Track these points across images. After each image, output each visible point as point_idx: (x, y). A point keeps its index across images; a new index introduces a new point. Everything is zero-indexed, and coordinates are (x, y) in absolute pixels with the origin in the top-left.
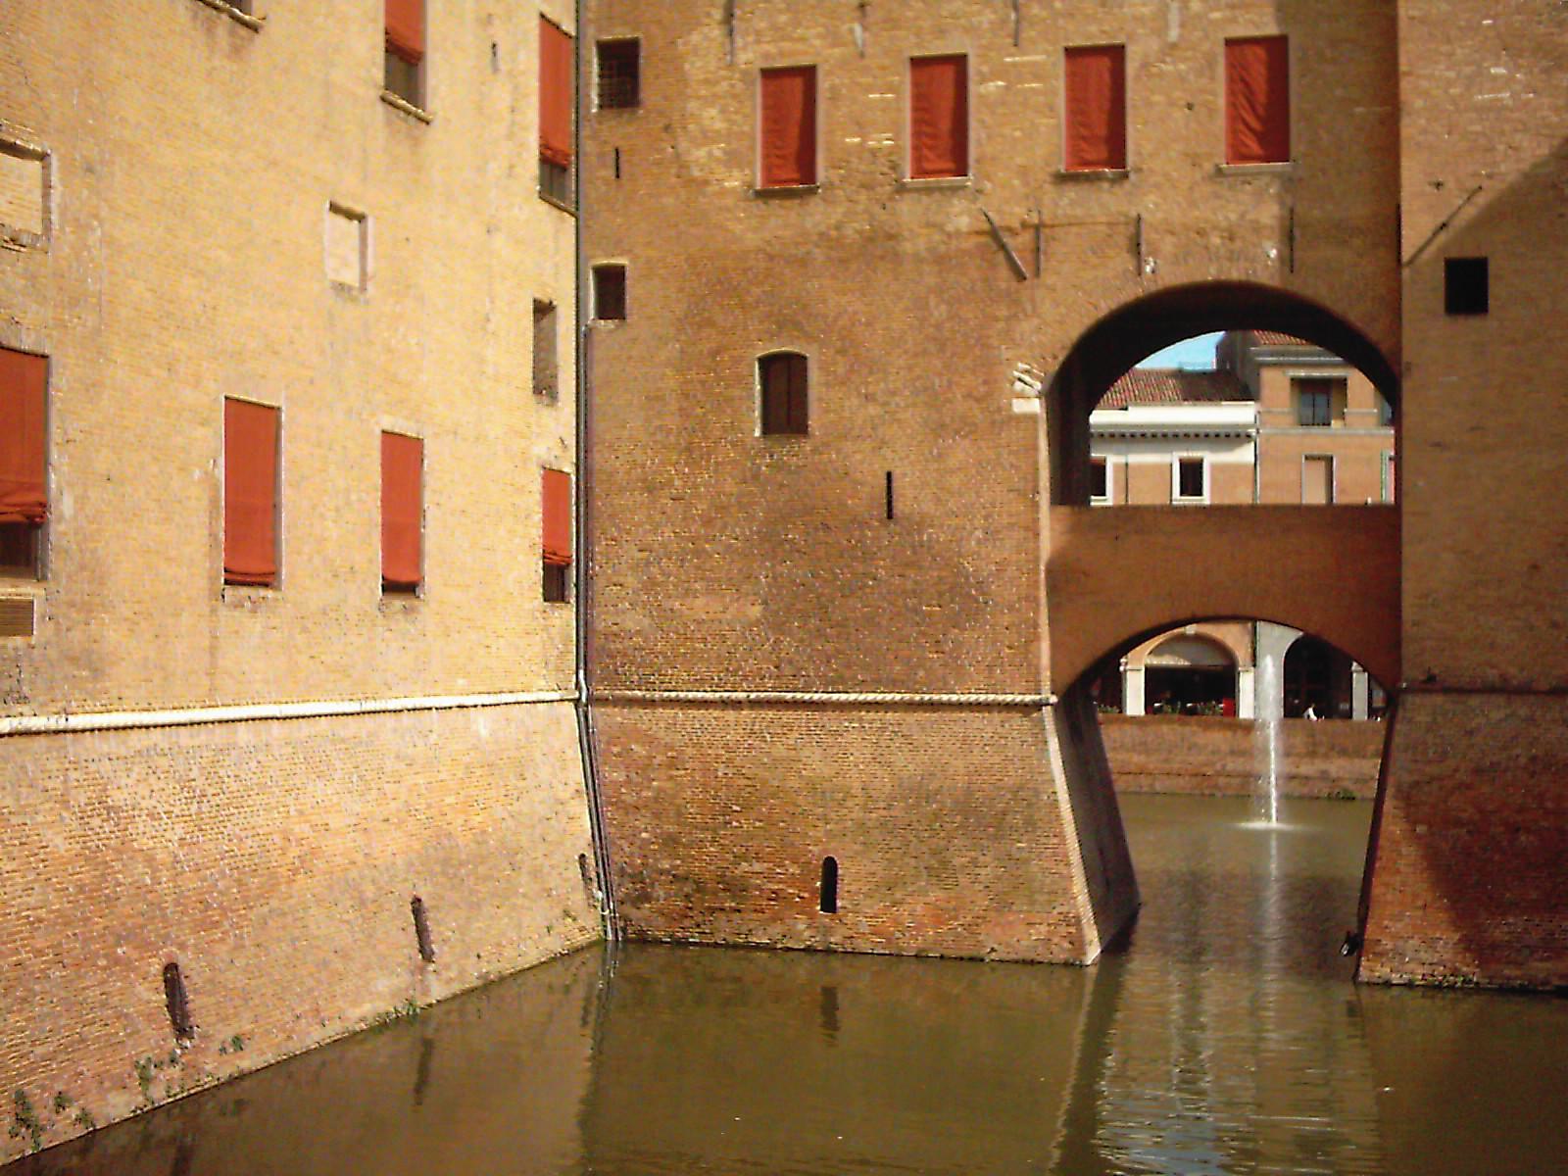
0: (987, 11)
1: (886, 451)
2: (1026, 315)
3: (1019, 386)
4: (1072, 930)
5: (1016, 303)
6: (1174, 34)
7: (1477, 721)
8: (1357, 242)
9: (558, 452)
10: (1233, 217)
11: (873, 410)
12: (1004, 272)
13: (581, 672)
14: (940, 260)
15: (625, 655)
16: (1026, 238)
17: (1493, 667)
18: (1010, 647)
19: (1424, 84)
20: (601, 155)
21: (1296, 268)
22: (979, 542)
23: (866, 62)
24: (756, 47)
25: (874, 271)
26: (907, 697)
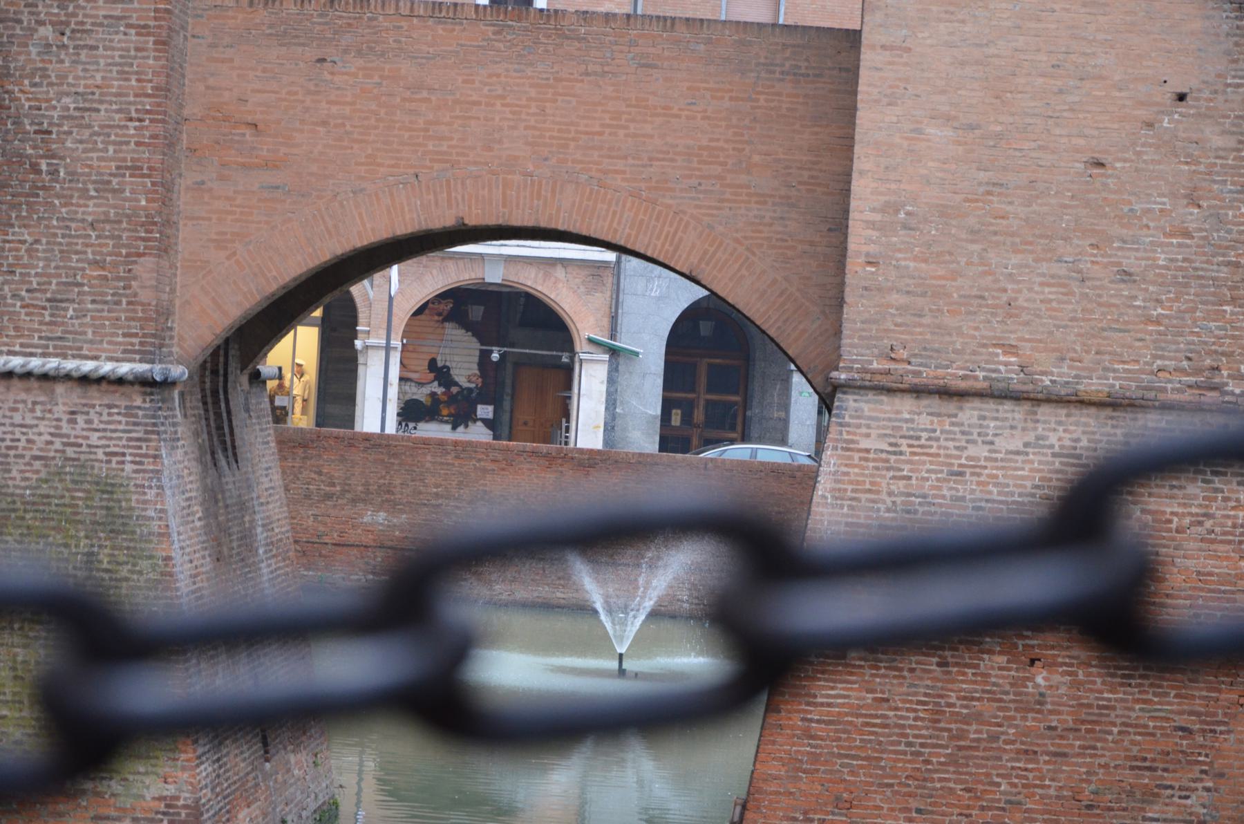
7: (972, 451)
17: (1011, 349)
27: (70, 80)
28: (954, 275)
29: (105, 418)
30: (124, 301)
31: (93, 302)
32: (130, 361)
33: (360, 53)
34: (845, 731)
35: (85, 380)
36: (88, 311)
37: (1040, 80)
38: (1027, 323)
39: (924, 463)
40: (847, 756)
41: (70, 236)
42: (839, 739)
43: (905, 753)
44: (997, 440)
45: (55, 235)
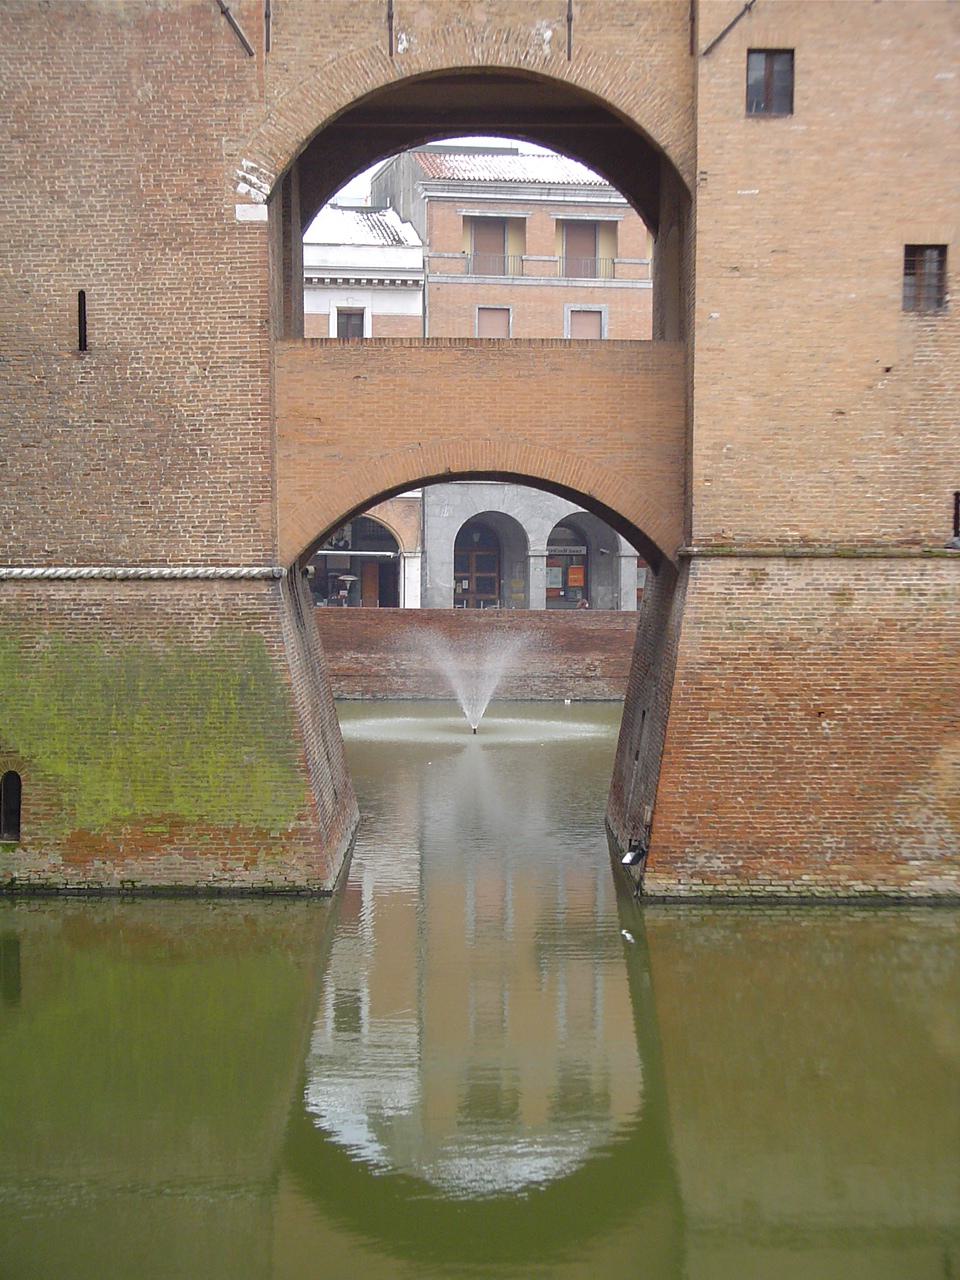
2: (252, 100)
3: (243, 188)
7: (775, 590)
12: (225, 44)
17: (794, 527)
21: (575, 52)
25: (60, 34)
27: (211, 398)
28: (758, 485)
29: (245, 602)
30: (252, 530)
31: (233, 531)
32: (257, 566)
33: (380, 371)
34: (711, 763)
35: (232, 579)
36: (231, 537)
37: (803, 365)
38: (804, 511)
39: (747, 598)
40: (713, 778)
41: (217, 492)
42: (707, 768)
43: (747, 773)
44: (789, 582)
45: (208, 492)
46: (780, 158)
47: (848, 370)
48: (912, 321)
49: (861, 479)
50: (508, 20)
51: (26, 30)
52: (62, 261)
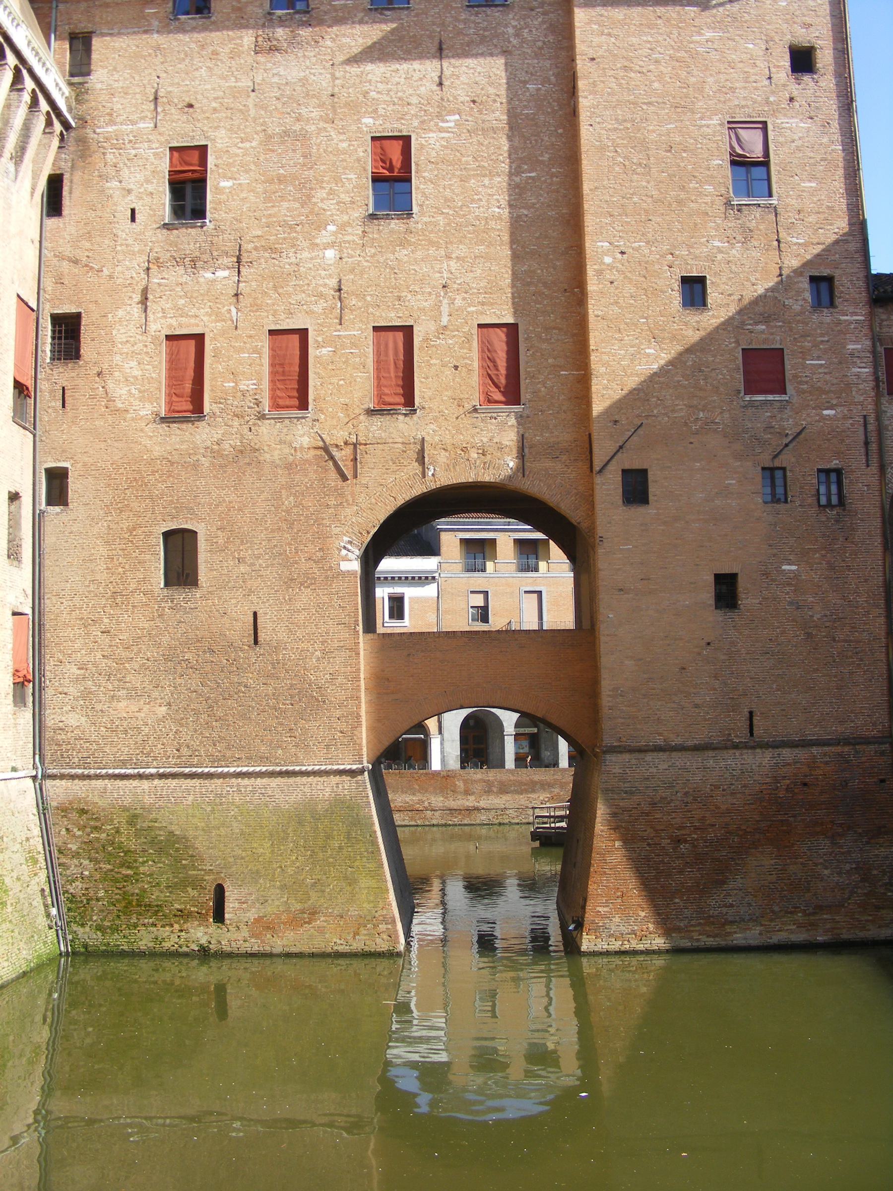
0: (321, 301)
1: (253, 597)
2: (349, 504)
3: (344, 552)
4: (389, 926)
5: (341, 495)
6: (445, 320)
7: (651, 770)
8: (564, 458)
9: (22, 599)
10: (485, 440)
11: (243, 569)
12: (333, 474)
13: (37, 757)
14: (289, 467)
15: (69, 743)
16: (348, 451)
17: (660, 734)
18: (342, 732)
19: (605, 358)
20: (52, 392)
21: (527, 473)
22: (318, 659)
23: (239, 332)
24: (163, 321)
26: (271, 768)
33: (422, 651)
37: (661, 642)
38: (666, 725)
46: (643, 528)
47: (687, 644)
48: (719, 616)
49: (697, 706)
50: (489, 457)
51: (225, 472)
52: (244, 595)
